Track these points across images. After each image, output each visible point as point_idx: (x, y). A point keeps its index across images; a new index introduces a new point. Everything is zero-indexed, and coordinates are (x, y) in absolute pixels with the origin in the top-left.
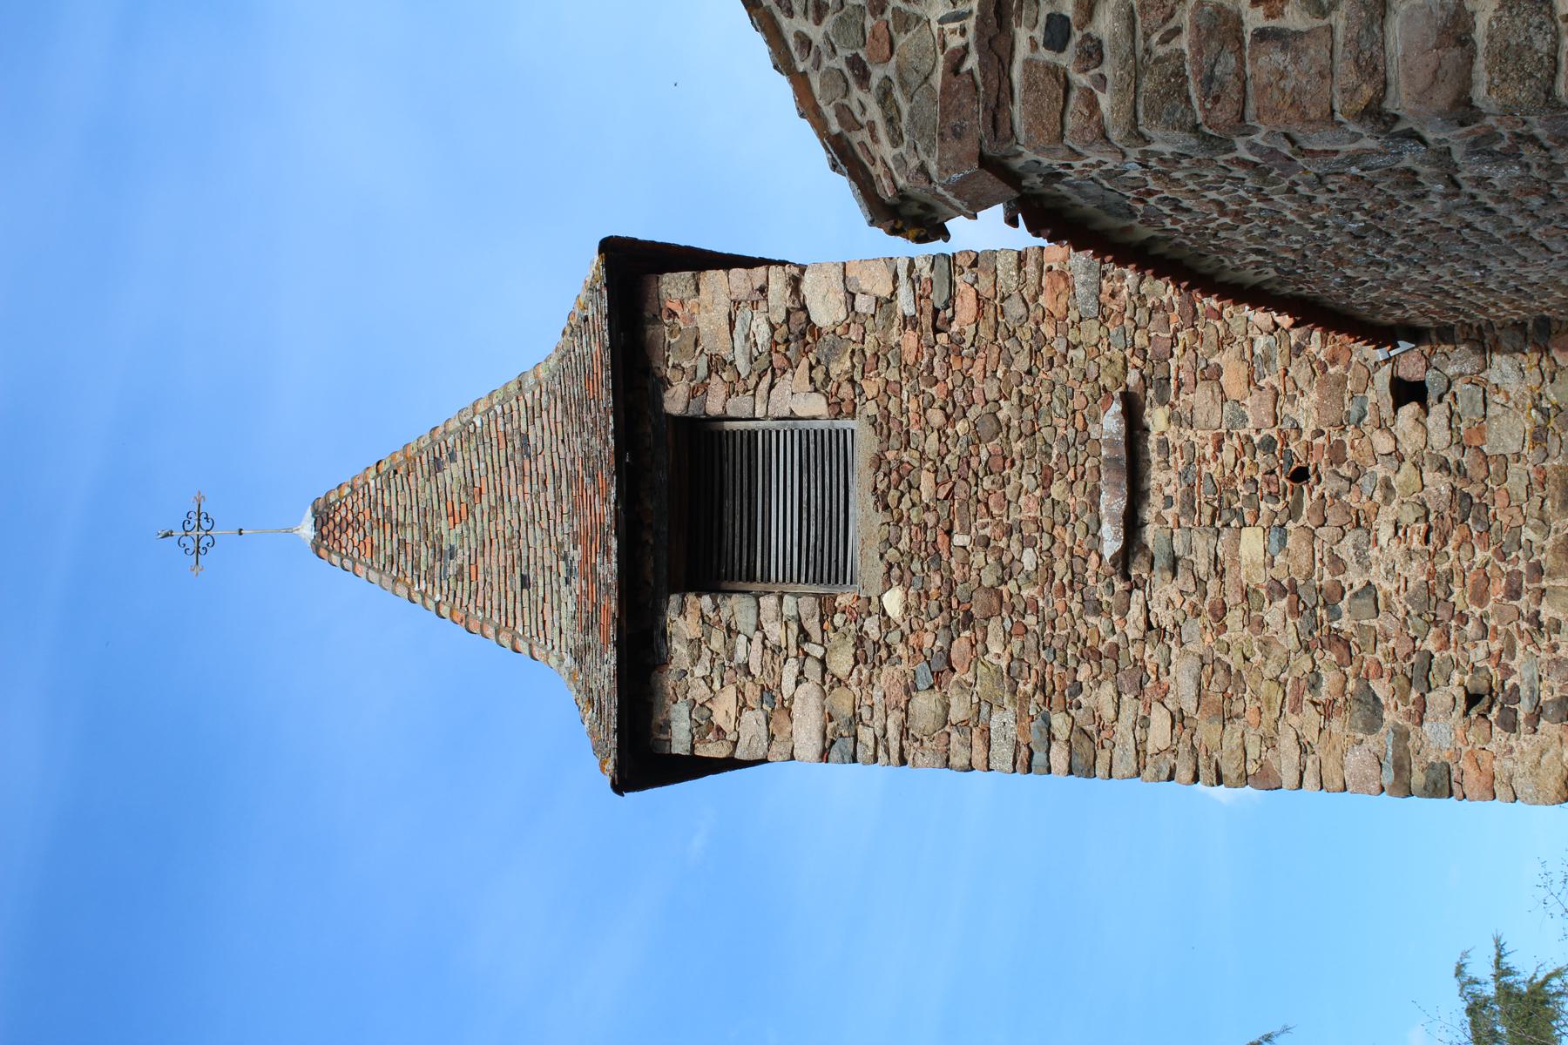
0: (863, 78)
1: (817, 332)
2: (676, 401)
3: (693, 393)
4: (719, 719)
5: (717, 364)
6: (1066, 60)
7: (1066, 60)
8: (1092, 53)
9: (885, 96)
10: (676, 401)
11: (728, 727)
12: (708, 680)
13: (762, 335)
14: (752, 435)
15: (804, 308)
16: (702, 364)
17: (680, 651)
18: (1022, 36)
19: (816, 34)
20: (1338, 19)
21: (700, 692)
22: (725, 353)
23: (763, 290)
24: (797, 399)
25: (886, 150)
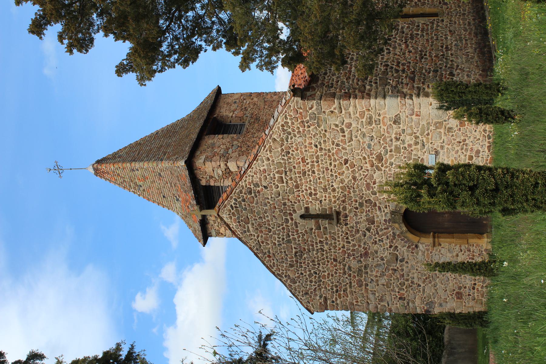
0: (309, 303)
1: (232, 173)
2: (203, 183)
3: (207, 182)
4: (221, 231)
5: (211, 177)
6: (334, 304)
7: (334, 304)
8: (337, 304)
9: (312, 305)
10: (203, 183)
11: (224, 233)
12: (218, 226)
13: (221, 173)
14: (218, 187)
15: (228, 168)
16: (208, 177)
17: (211, 222)
18: (329, 302)
19: (303, 298)
20: (364, 305)
21: (217, 228)
22: (213, 175)
23: (220, 166)
24: (228, 182)
25: (312, 308)
